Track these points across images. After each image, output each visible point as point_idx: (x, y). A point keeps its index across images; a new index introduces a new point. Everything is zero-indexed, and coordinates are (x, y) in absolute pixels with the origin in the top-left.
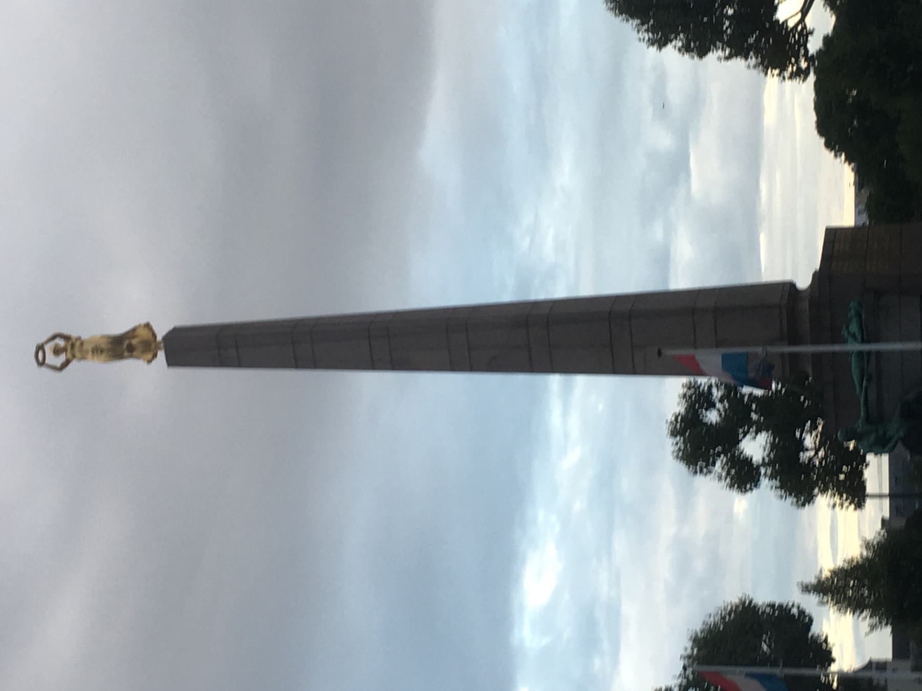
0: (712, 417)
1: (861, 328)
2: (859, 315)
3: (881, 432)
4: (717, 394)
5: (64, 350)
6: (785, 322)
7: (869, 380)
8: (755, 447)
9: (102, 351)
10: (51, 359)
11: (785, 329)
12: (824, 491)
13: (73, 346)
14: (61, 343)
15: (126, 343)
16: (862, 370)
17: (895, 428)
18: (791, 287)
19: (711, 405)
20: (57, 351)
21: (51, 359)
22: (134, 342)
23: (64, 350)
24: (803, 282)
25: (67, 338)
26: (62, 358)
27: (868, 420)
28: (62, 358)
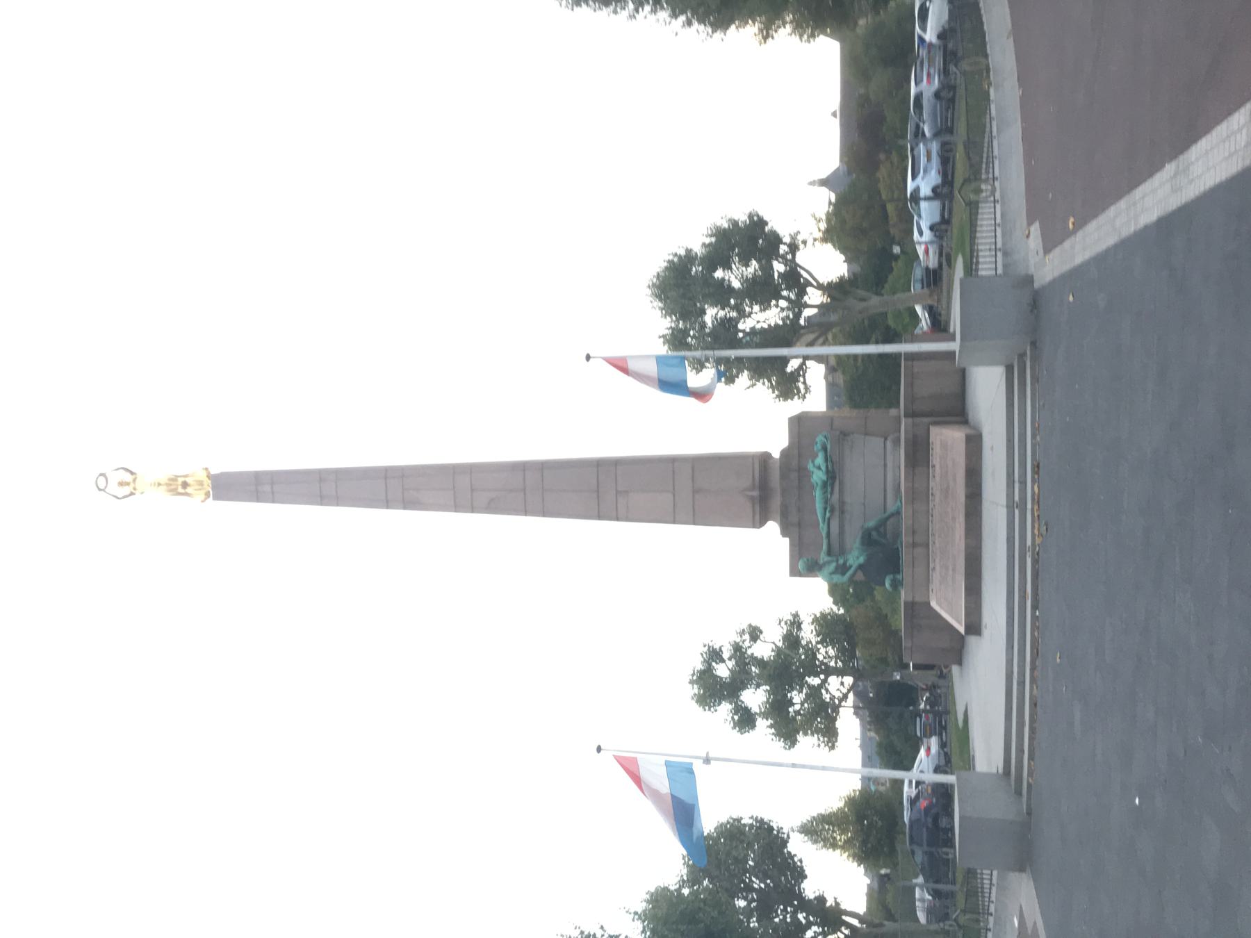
0: (723, 671)
1: (826, 460)
2: (825, 449)
3: (841, 561)
4: (726, 655)
5: (128, 484)
6: (757, 475)
7: (832, 511)
8: (755, 698)
9: (159, 484)
10: (113, 488)
12: (806, 734)
13: (134, 480)
14: (129, 478)
15: (180, 480)
16: (826, 502)
17: (855, 558)
18: (765, 458)
19: (723, 661)
20: (121, 484)
21: (113, 488)
22: (188, 480)
23: (128, 484)
24: (776, 455)
25: (132, 473)
26: (127, 490)
27: (829, 553)
28: (127, 490)
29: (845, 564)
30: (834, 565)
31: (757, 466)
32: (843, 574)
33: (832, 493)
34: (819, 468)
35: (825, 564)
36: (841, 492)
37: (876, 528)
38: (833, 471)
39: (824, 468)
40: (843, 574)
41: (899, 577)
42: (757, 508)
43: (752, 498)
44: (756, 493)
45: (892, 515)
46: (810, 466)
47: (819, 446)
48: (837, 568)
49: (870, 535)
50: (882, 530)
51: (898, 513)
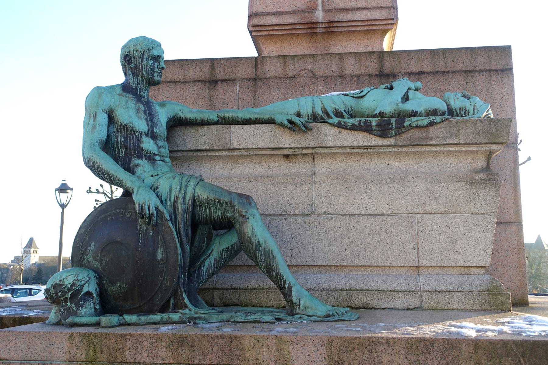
3: (148, 144)
6: (363, 15)
11: (349, 17)
16: (315, 118)
29: (150, 158)
30: (141, 125)
31: (375, 15)
32: (107, 146)
33: (339, 125)
34: (406, 98)
35: (148, 104)
36: (349, 152)
37: (245, 246)
38: (400, 129)
39: (409, 106)
40: (107, 146)
41: (86, 312)
42: (290, 20)
43: (312, 9)
44: (320, 15)
45: (286, 291)
46: (402, 85)
47: (457, 102)
48: (127, 130)
49: (227, 225)
50: (243, 259)
51: (290, 308)
